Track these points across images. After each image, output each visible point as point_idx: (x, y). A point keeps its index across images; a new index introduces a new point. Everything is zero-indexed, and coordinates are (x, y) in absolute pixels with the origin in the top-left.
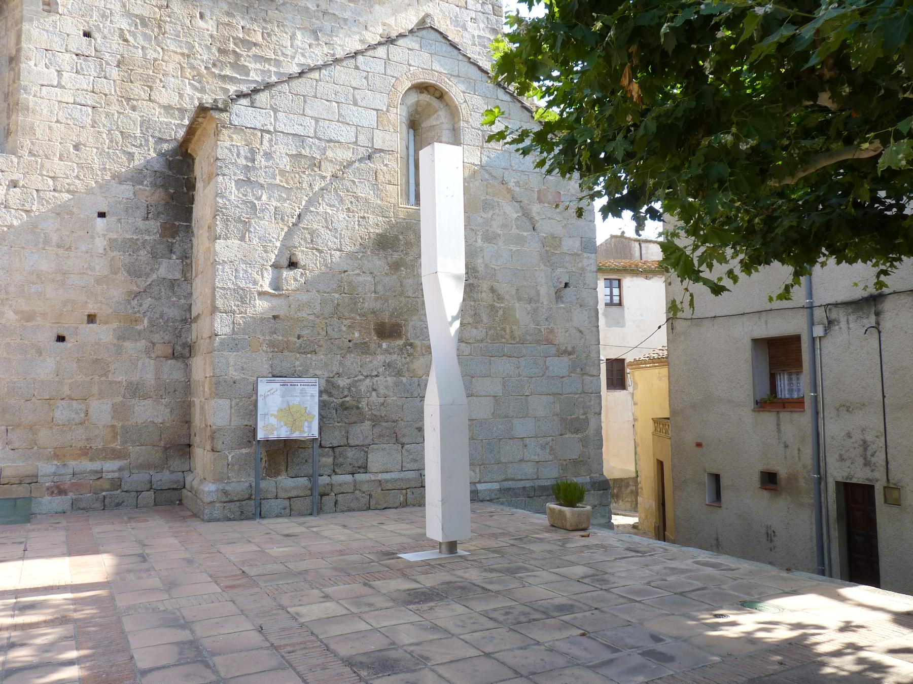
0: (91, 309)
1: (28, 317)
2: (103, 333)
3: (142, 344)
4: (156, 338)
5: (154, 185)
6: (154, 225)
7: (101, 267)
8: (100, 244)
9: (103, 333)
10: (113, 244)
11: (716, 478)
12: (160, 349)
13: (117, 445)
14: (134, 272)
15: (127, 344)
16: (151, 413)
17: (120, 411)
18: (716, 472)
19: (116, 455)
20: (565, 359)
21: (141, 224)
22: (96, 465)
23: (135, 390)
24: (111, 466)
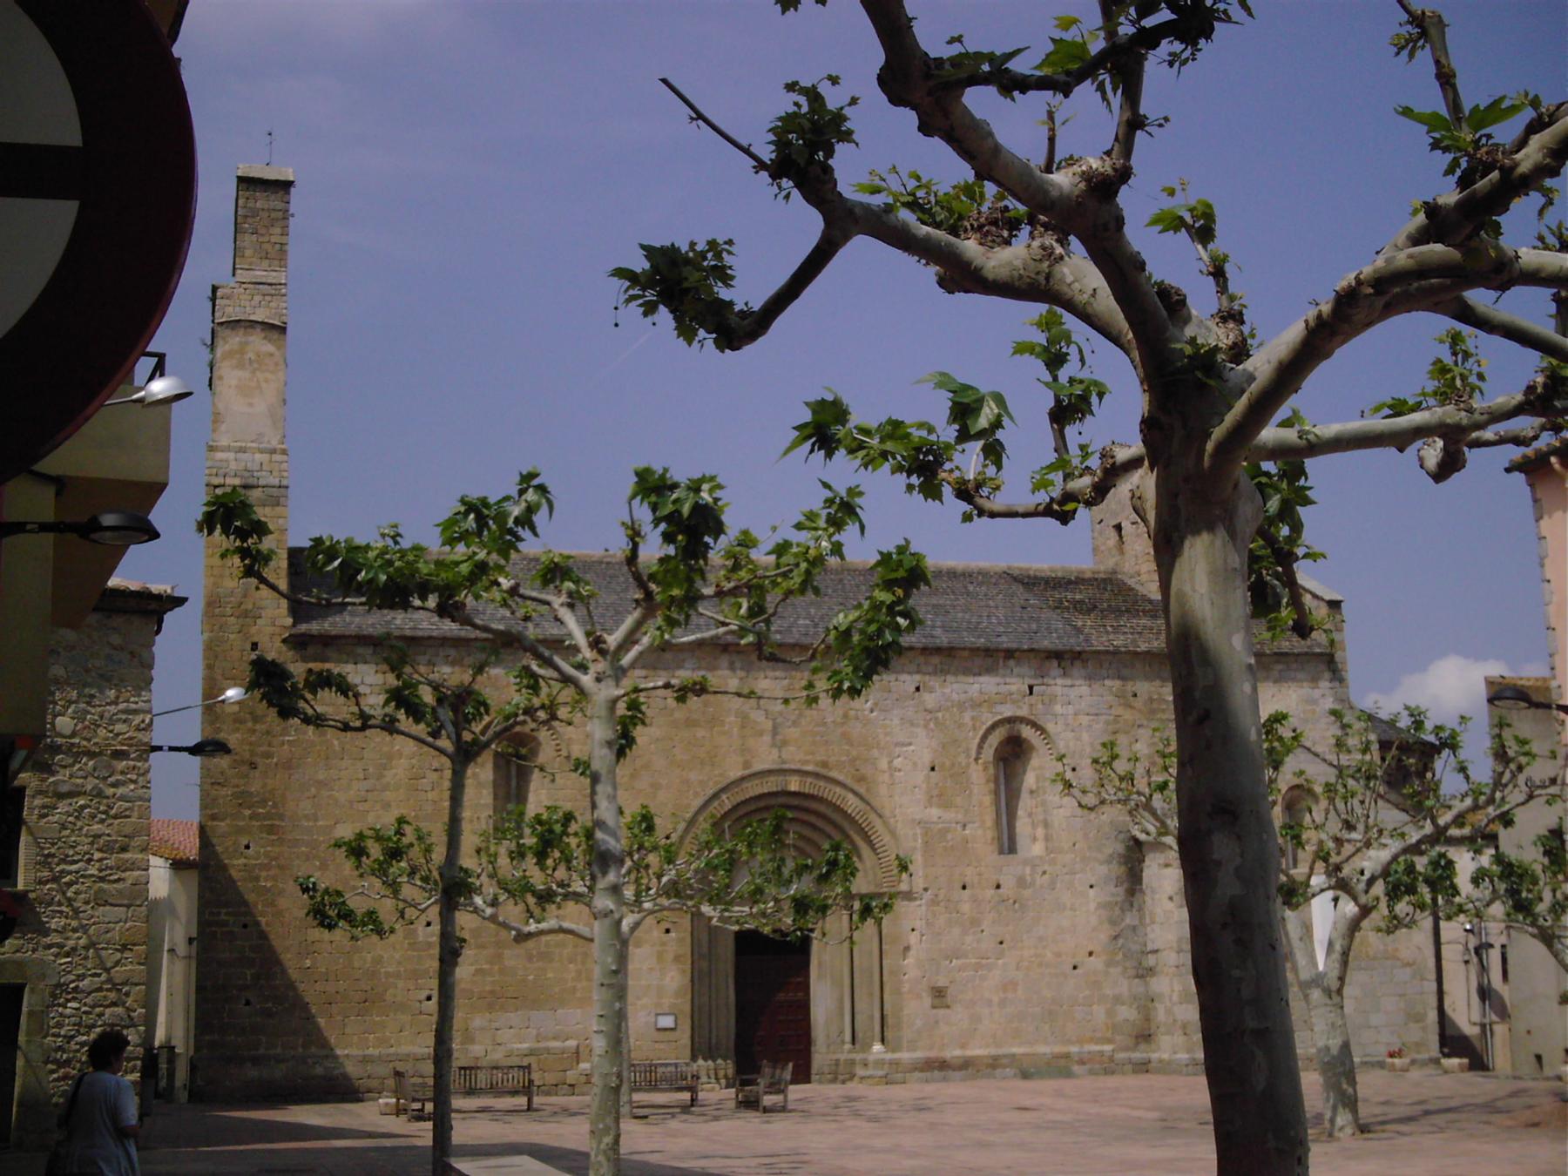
0: (1090, 948)
1: (1058, 955)
2: (1096, 963)
3: (1119, 969)
4: (1128, 964)
5: (1120, 863)
6: (1121, 890)
7: (1094, 920)
8: (1092, 906)
9: (1096, 963)
10: (1100, 906)
11: (1539, 1058)
12: (1132, 972)
13: (1109, 1035)
14: (1113, 923)
15: (1112, 970)
16: (1127, 1013)
17: (1110, 1013)
18: (1540, 1052)
19: (1109, 1041)
20: (1408, 970)
21: (1114, 890)
22: (1098, 1048)
23: (1117, 1000)
24: (1108, 1048)
